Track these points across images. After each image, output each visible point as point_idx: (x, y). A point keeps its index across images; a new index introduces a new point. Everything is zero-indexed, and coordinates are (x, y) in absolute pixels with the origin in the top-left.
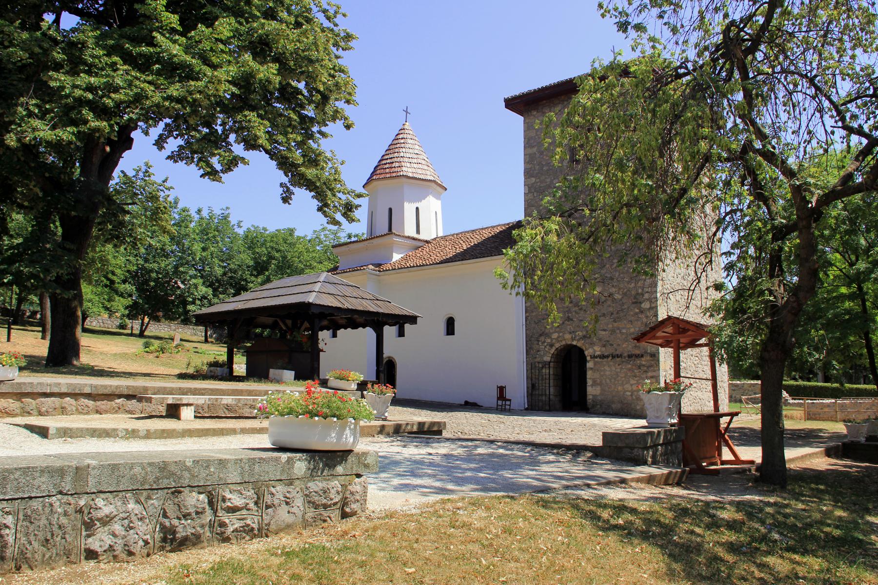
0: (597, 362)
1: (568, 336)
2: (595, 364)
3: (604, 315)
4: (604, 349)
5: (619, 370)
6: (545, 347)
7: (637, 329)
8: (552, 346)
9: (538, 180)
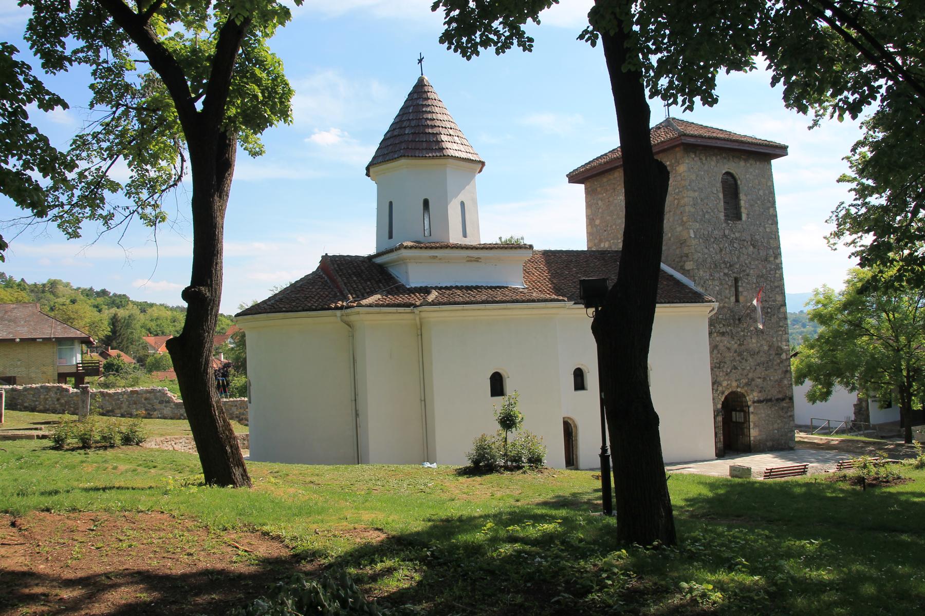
0: (756, 406)
1: (734, 384)
2: (754, 408)
3: (759, 365)
4: (760, 394)
5: (770, 412)
6: (719, 395)
7: (779, 377)
8: (723, 393)
9: (701, 227)
